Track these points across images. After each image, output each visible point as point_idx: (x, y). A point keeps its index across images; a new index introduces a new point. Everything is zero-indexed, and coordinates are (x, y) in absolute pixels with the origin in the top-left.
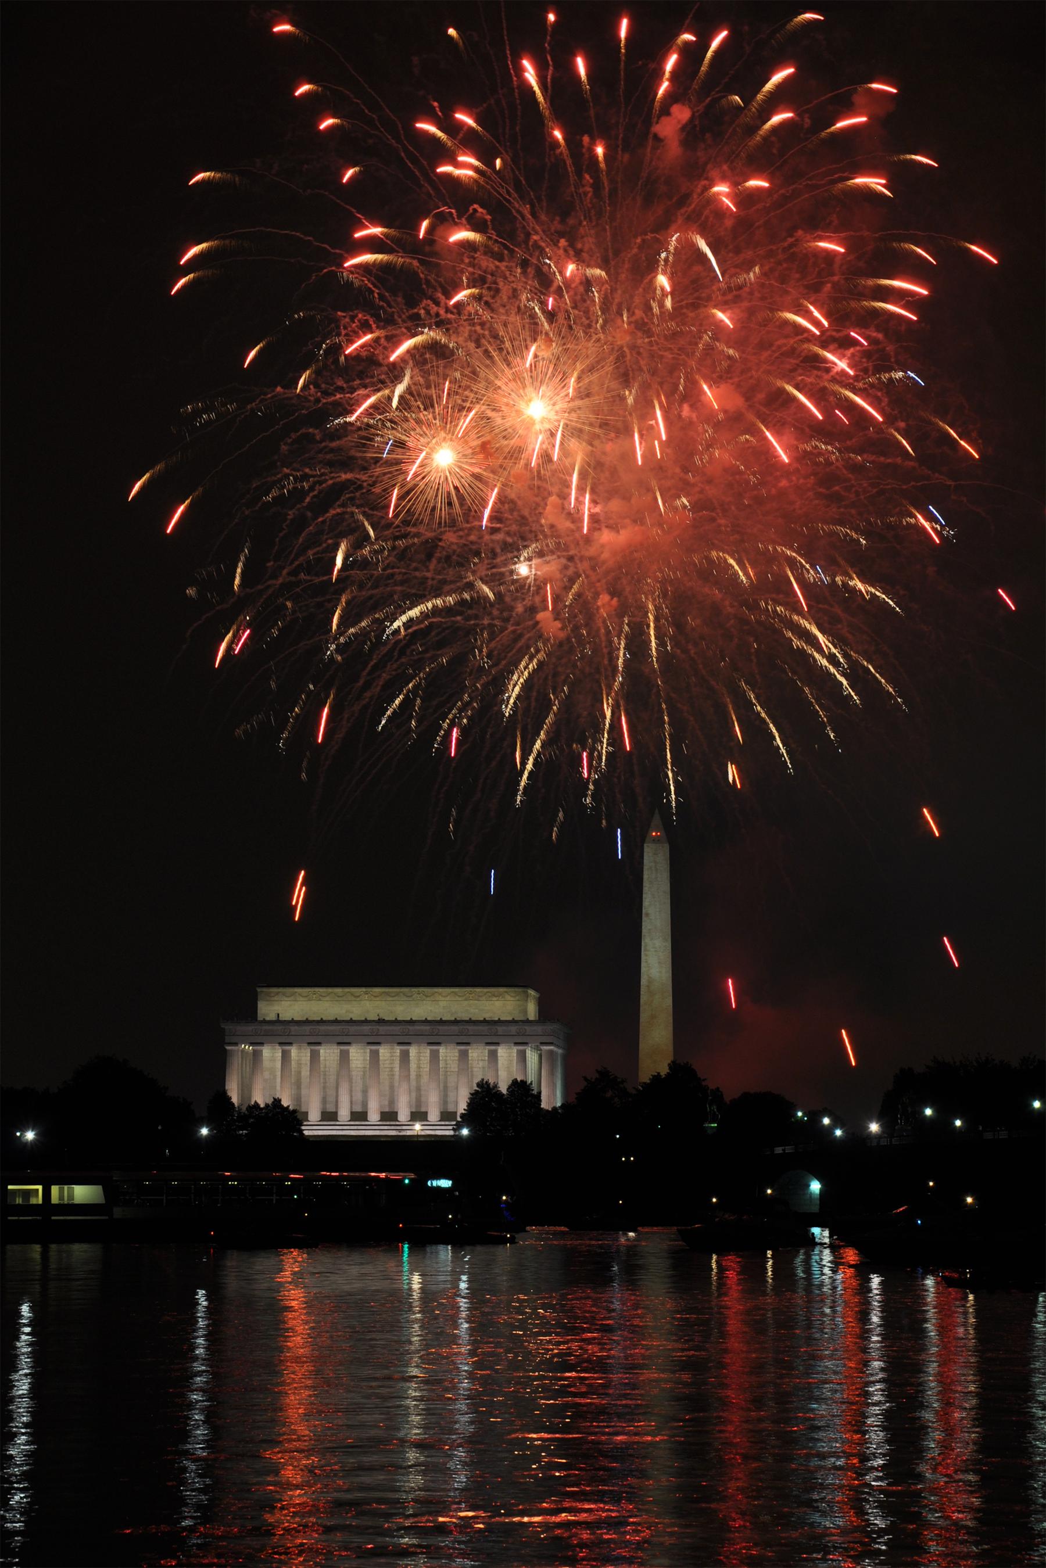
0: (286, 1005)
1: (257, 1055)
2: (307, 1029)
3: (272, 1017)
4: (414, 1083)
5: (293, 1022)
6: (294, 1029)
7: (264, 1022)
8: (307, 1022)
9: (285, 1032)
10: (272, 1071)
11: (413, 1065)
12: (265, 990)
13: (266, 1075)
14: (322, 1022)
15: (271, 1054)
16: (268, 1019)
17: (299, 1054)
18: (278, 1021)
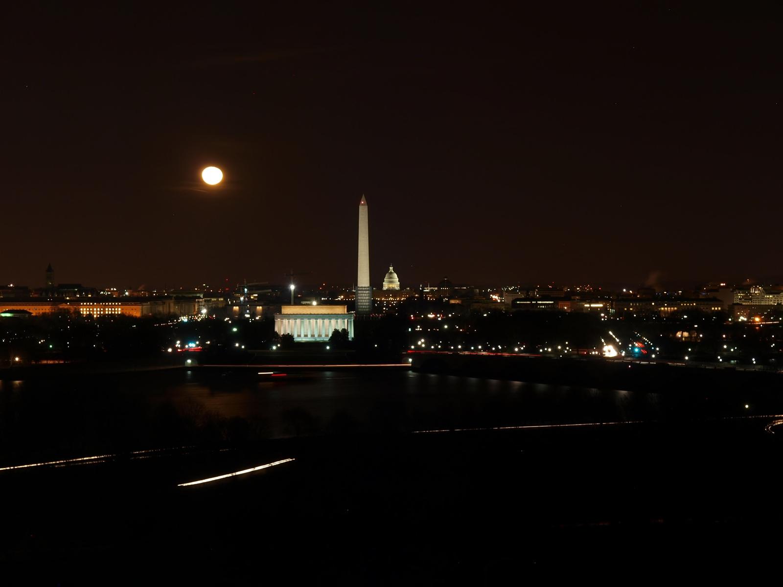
1: (282, 322)
2: (294, 316)
6: (291, 316)
7: (284, 314)
8: (294, 314)
9: (289, 316)
11: (318, 324)
14: (297, 314)
15: (285, 321)
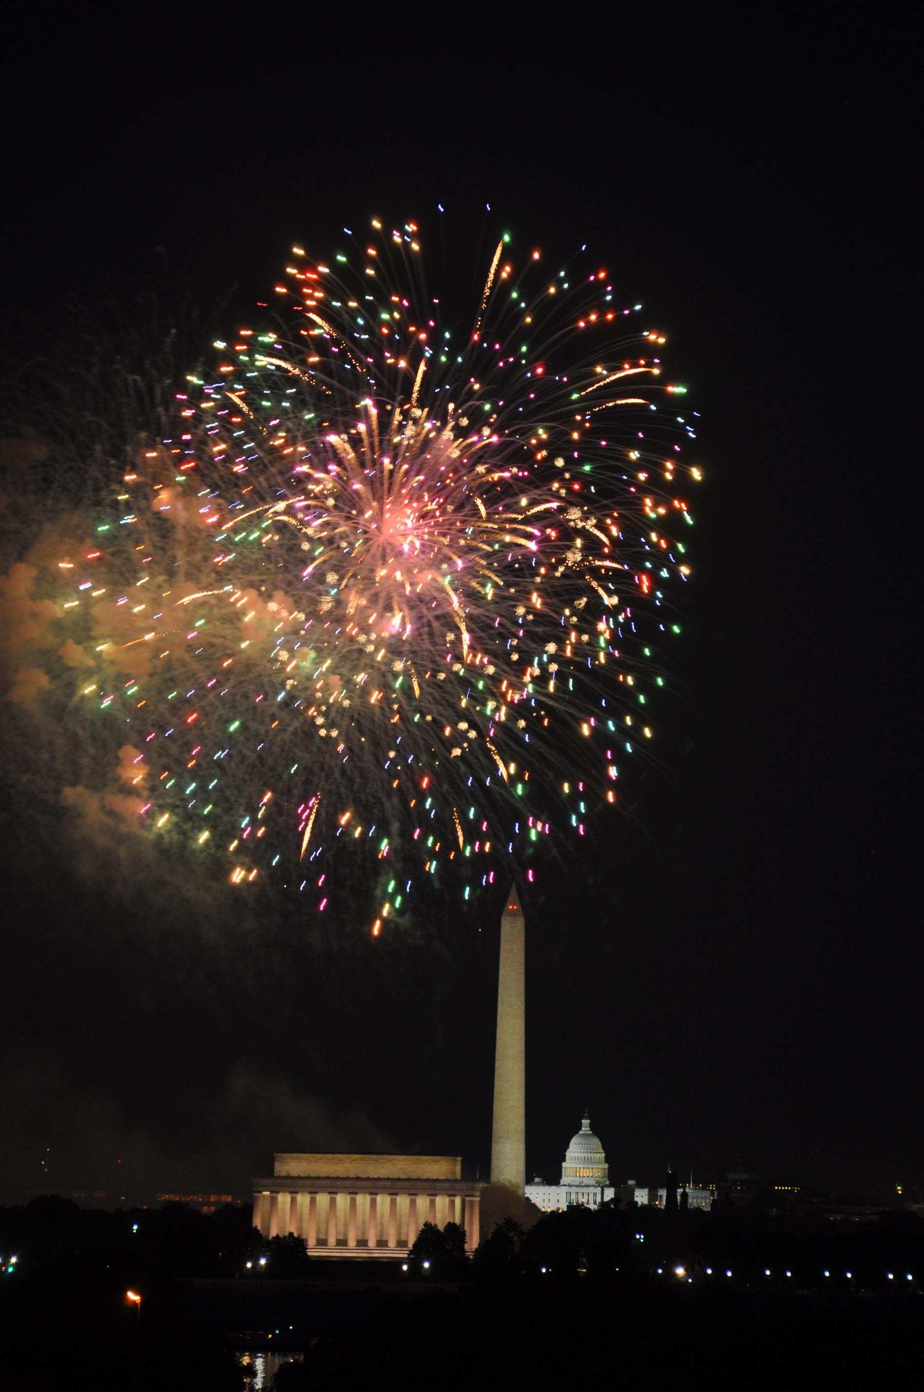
0: (293, 1165)
1: (273, 1201)
2: (308, 1182)
3: (283, 1174)
4: (378, 1220)
5: (299, 1178)
6: (299, 1182)
7: (280, 1177)
8: (309, 1178)
9: (294, 1185)
10: (284, 1211)
11: (378, 1208)
12: (280, 1155)
13: (280, 1213)
14: (318, 1178)
15: (284, 1199)
16: (282, 1175)
17: (303, 1199)
18: (288, 1177)
